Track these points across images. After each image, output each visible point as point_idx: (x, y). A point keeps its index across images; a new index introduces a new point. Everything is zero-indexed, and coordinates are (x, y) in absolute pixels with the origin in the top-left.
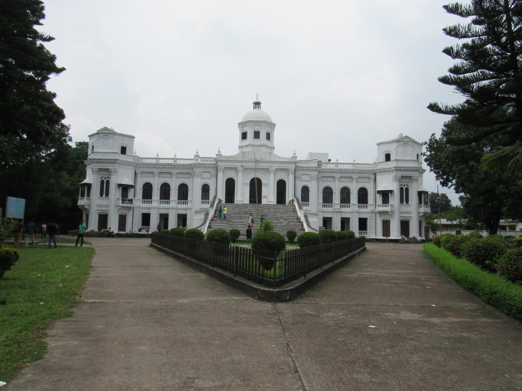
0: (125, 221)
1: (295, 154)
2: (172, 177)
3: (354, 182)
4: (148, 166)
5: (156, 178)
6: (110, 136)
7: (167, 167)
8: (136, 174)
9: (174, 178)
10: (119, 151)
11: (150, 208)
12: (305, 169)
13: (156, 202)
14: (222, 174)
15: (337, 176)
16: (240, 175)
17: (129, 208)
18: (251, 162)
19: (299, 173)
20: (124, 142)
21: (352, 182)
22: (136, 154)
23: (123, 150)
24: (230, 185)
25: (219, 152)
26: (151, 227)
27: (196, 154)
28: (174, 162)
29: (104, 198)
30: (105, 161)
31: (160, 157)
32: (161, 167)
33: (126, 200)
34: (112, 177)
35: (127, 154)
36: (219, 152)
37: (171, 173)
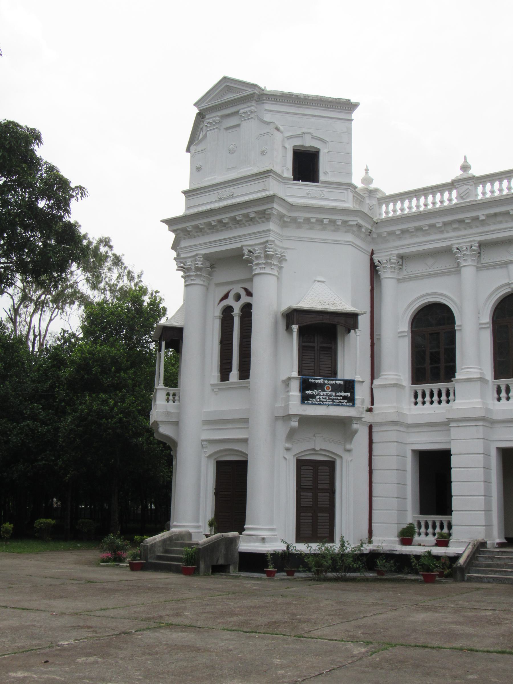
0: (332, 492)
4: (424, 223)
5: (468, 272)
6: (243, 109)
8: (374, 270)
10: (287, 168)
11: (445, 425)
13: (478, 384)
17: (343, 426)
20: (309, 131)
22: (372, 186)
23: (306, 165)
26: (455, 518)
29: (234, 387)
30: (225, 217)
31: (476, 171)
33: (321, 387)
34: (257, 280)
35: (322, 177)
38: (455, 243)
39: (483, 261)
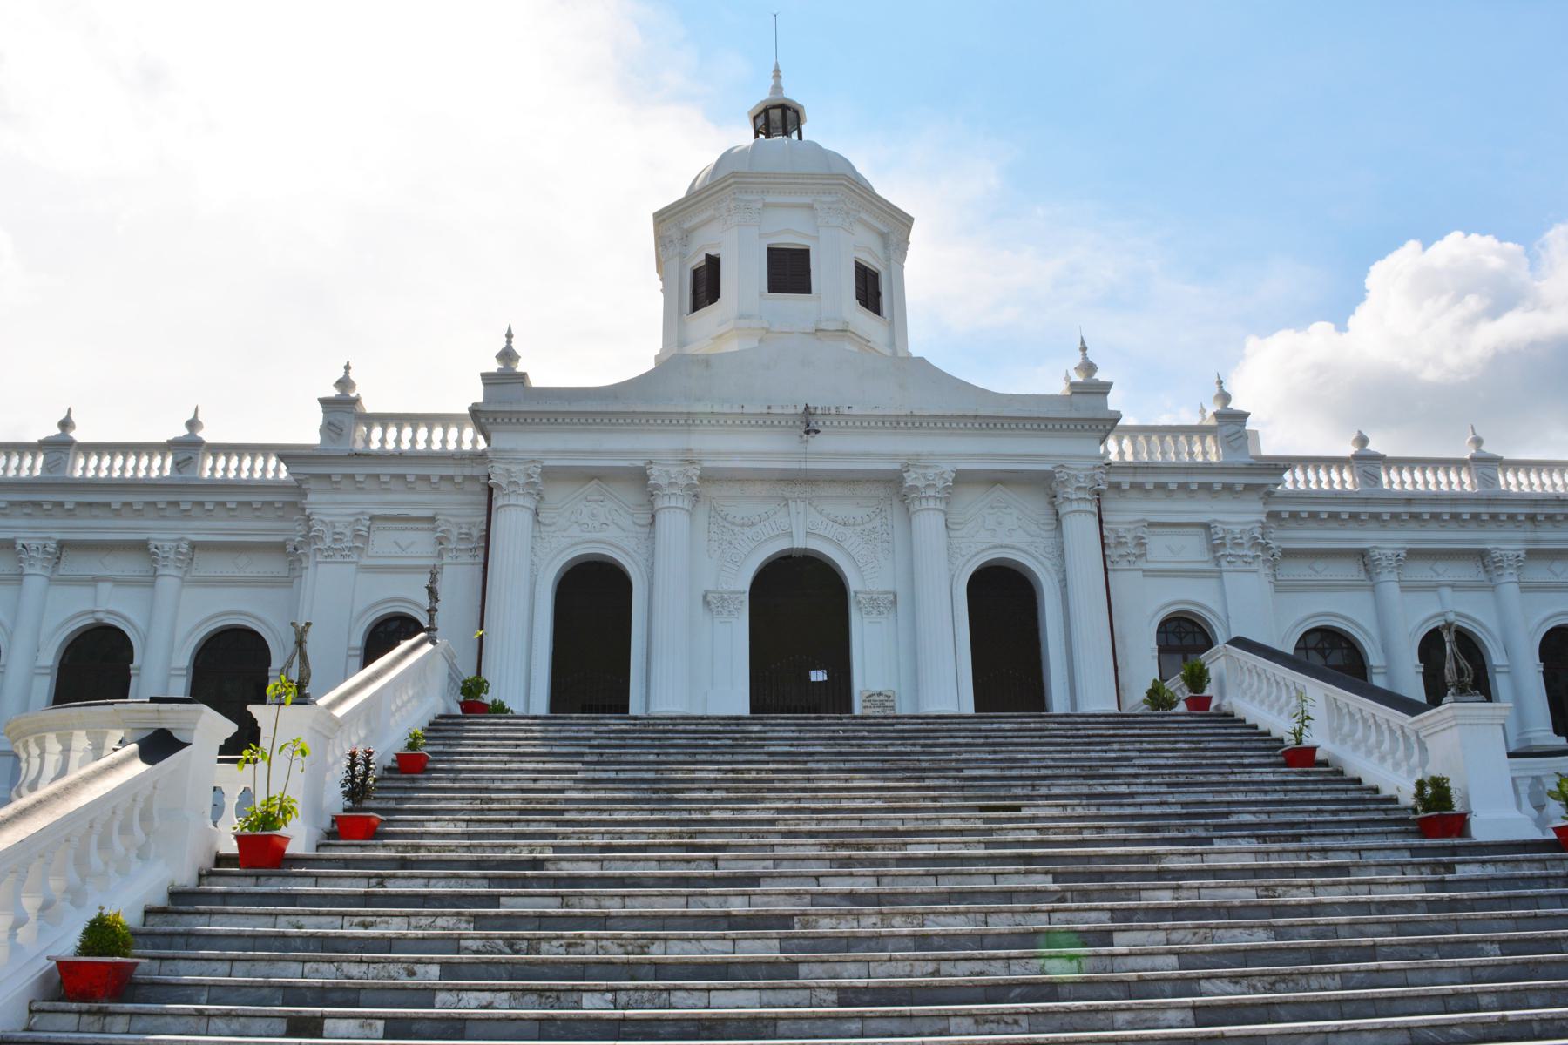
1: (1089, 367)
2: (151, 580)
3: (1509, 589)
7: (116, 500)
9: (168, 583)
12: (1173, 481)
14: (526, 518)
15: (1386, 541)
16: (674, 522)
18: (766, 420)
19: (1126, 514)
21: (1493, 588)
24: (594, 607)
25: (507, 356)
27: (333, 392)
28: (177, 465)
32: (70, 499)
36: (507, 356)
37: (142, 547)
38: (22, 537)
39: (62, 572)
